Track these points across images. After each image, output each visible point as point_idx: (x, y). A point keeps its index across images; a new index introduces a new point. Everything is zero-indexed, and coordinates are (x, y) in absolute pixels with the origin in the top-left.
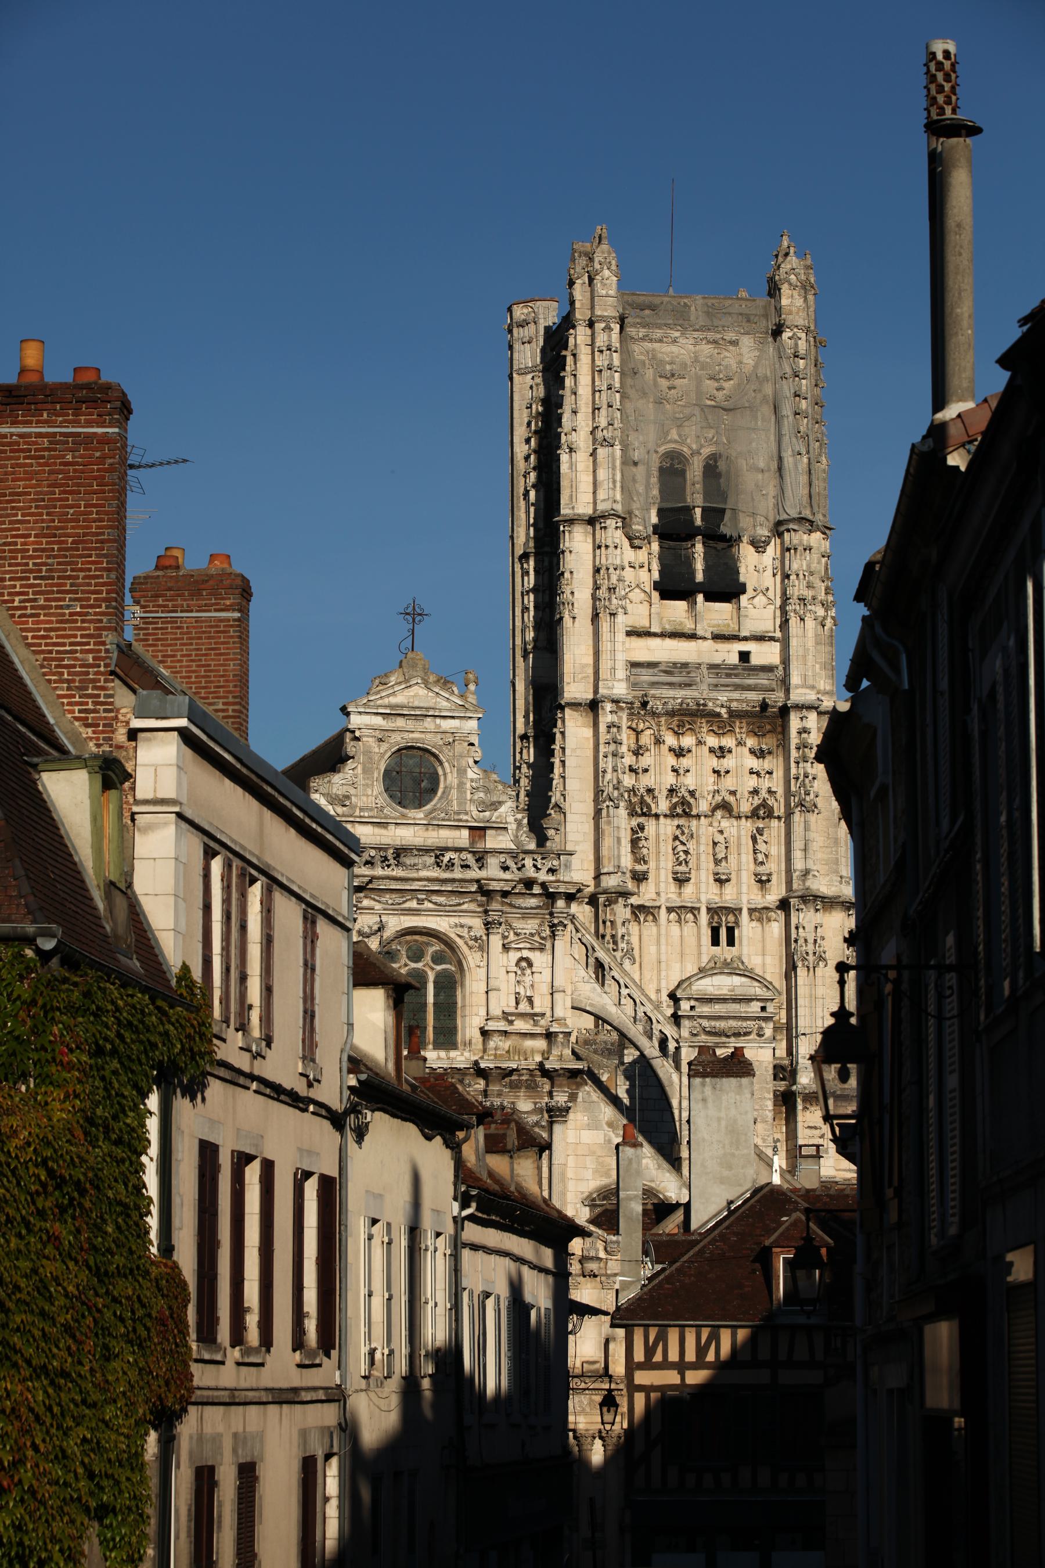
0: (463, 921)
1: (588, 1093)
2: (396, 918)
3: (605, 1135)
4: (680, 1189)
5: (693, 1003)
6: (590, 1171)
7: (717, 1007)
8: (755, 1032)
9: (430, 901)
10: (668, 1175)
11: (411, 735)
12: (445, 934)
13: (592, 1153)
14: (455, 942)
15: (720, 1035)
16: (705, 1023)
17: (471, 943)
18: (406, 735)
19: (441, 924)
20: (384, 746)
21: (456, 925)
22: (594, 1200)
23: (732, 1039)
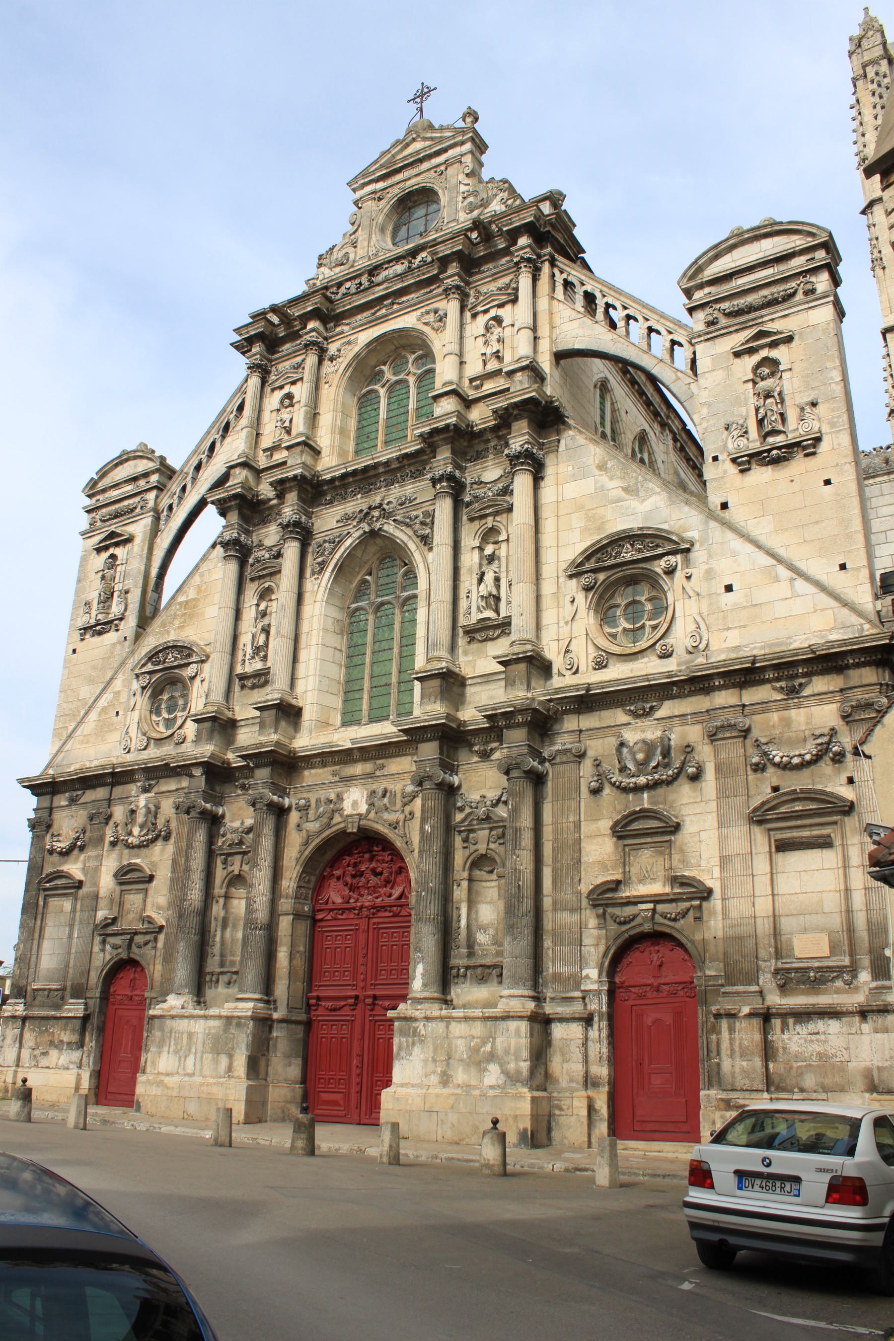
0: (427, 308)
1: (573, 438)
2: (365, 332)
3: (596, 482)
4: (706, 523)
5: (707, 290)
6: (578, 531)
7: (741, 281)
8: (800, 292)
9: (399, 304)
10: (686, 509)
11: (409, 183)
12: (413, 329)
13: (580, 508)
14: (423, 333)
15: (749, 312)
16: (725, 305)
17: (436, 325)
18: (401, 185)
19: (408, 321)
20: (383, 202)
21: (422, 315)
22: (581, 564)
23: (764, 312)
